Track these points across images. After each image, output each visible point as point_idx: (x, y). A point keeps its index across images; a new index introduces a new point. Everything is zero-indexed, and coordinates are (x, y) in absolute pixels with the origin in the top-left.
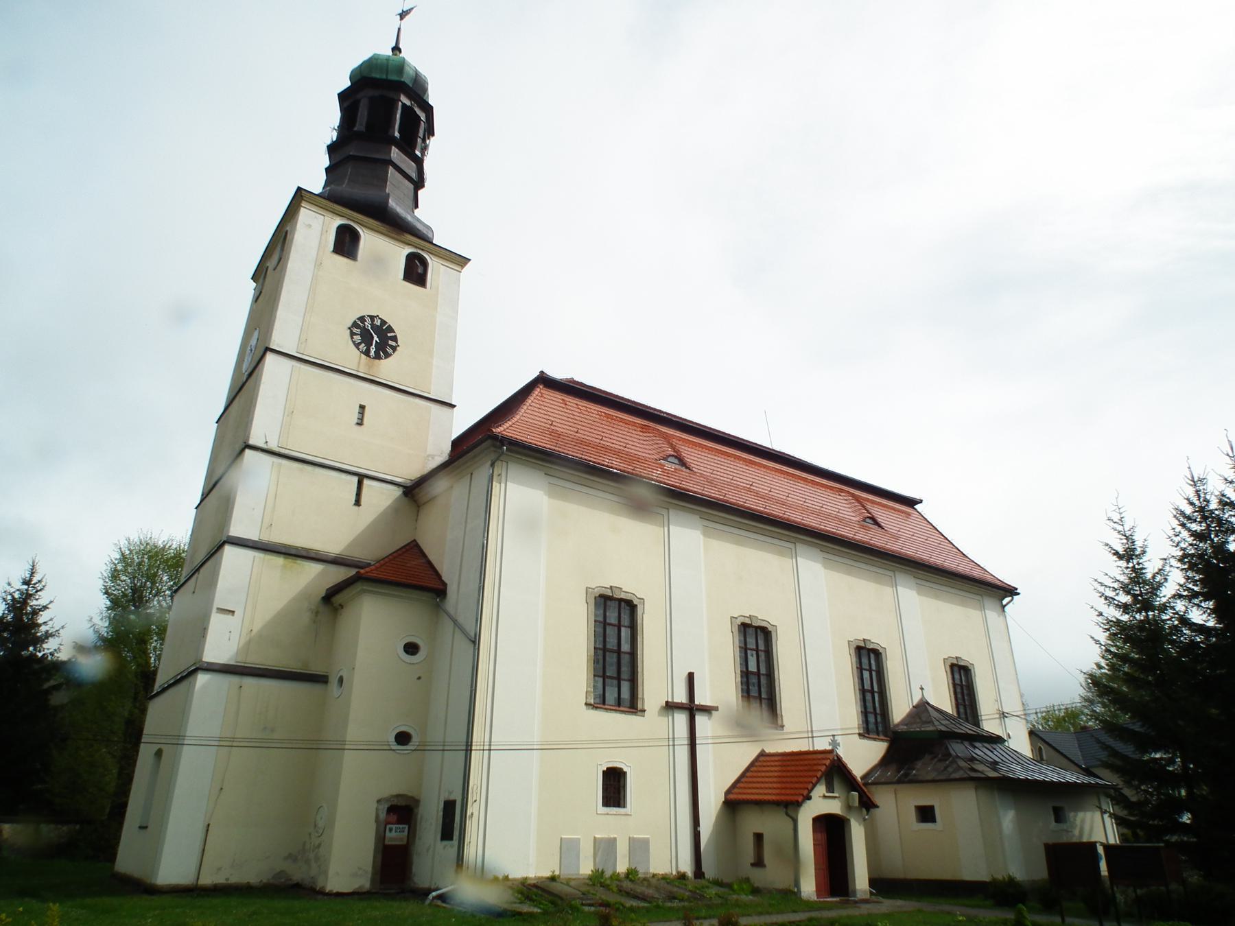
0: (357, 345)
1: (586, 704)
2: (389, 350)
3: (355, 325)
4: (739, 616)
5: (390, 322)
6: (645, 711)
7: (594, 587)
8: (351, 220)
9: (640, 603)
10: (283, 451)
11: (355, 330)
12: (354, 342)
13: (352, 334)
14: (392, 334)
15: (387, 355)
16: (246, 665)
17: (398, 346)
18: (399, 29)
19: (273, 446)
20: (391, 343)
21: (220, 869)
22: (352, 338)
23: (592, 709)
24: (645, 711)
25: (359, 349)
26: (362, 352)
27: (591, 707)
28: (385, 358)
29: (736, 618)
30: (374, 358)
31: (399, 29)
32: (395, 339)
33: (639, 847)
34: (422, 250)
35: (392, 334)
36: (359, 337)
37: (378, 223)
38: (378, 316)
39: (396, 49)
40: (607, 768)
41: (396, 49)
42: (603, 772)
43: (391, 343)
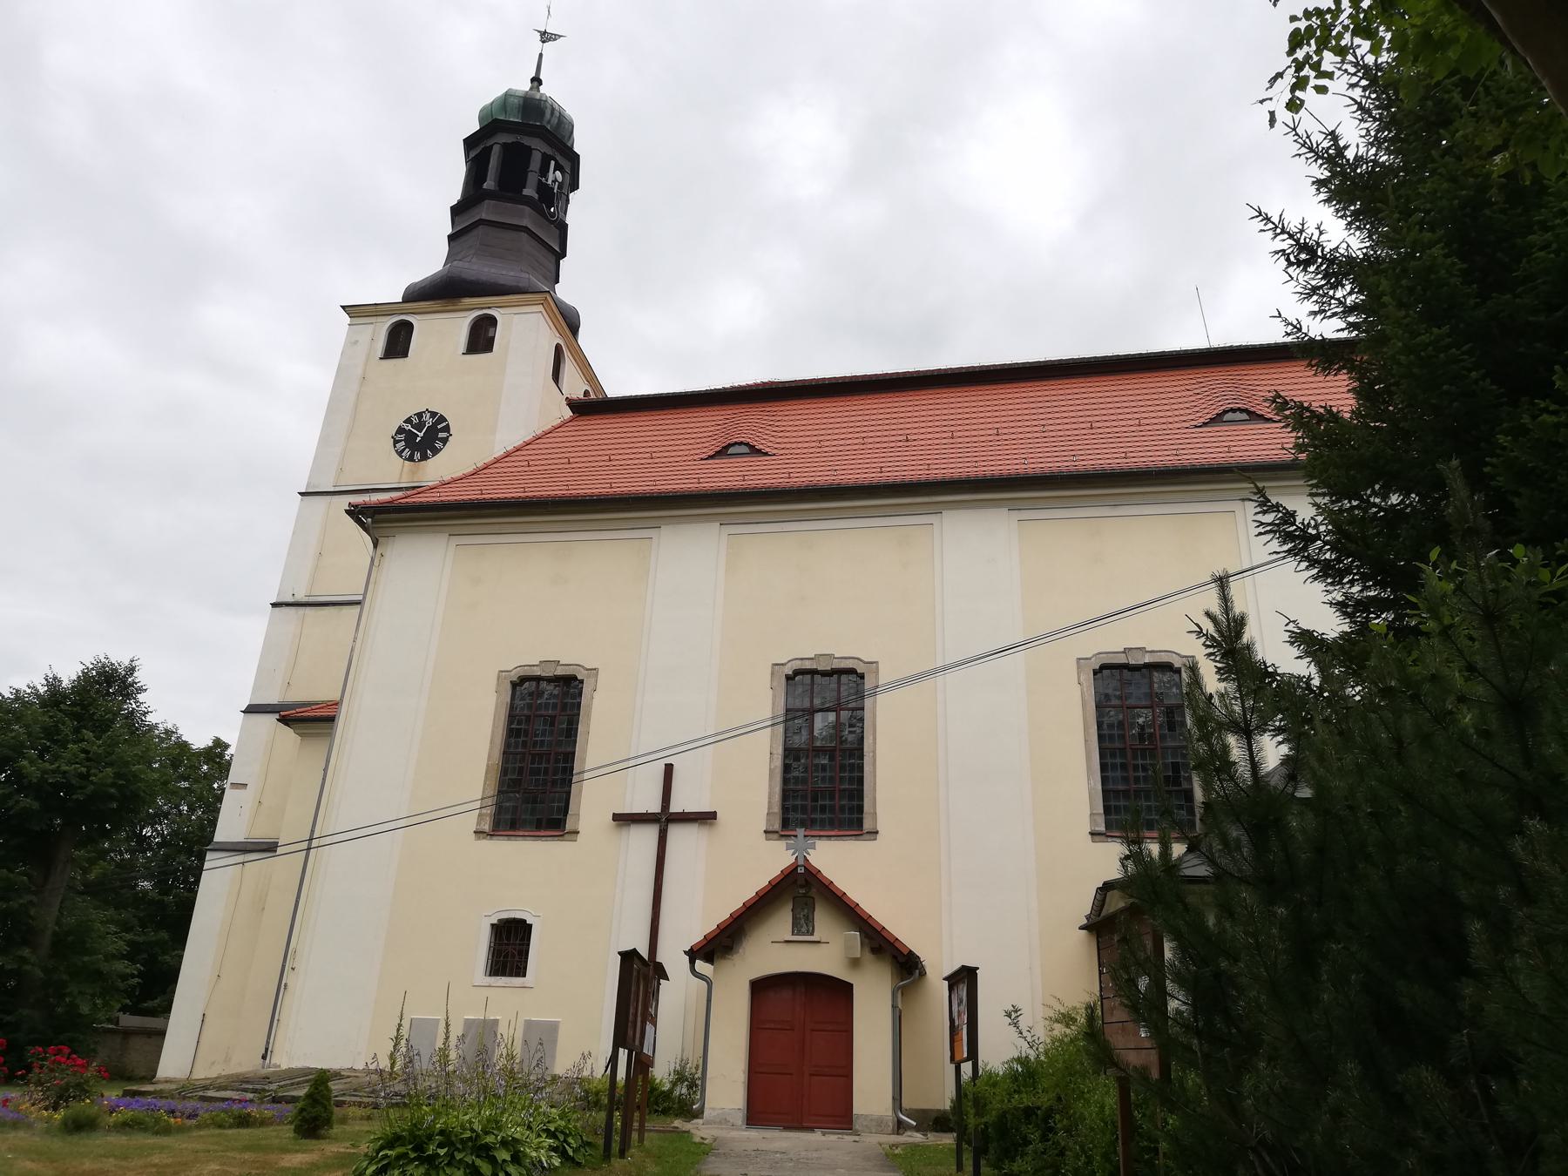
0: (400, 453)
1: (475, 832)
2: (438, 445)
3: (400, 430)
4: (789, 661)
5: (441, 411)
6: (578, 832)
7: (511, 669)
8: (402, 314)
9: (589, 676)
10: (311, 599)
11: (399, 437)
12: (396, 451)
13: (396, 442)
14: (444, 424)
15: (436, 451)
16: (249, 840)
17: (451, 435)
18: (541, 55)
19: (301, 597)
20: (441, 435)
21: (213, 1063)
22: (395, 447)
23: (484, 838)
24: (578, 832)
25: (401, 457)
26: (406, 459)
27: (481, 835)
28: (433, 456)
29: (782, 664)
30: (419, 461)
31: (541, 55)
32: (447, 429)
33: (543, 1036)
34: (489, 308)
35: (444, 424)
36: (403, 443)
37: (433, 302)
38: (427, 410)
39: (536, 81)
40: (499, 920)
41: (536, 81)
42: (493, 925)
43: (441, 435)
